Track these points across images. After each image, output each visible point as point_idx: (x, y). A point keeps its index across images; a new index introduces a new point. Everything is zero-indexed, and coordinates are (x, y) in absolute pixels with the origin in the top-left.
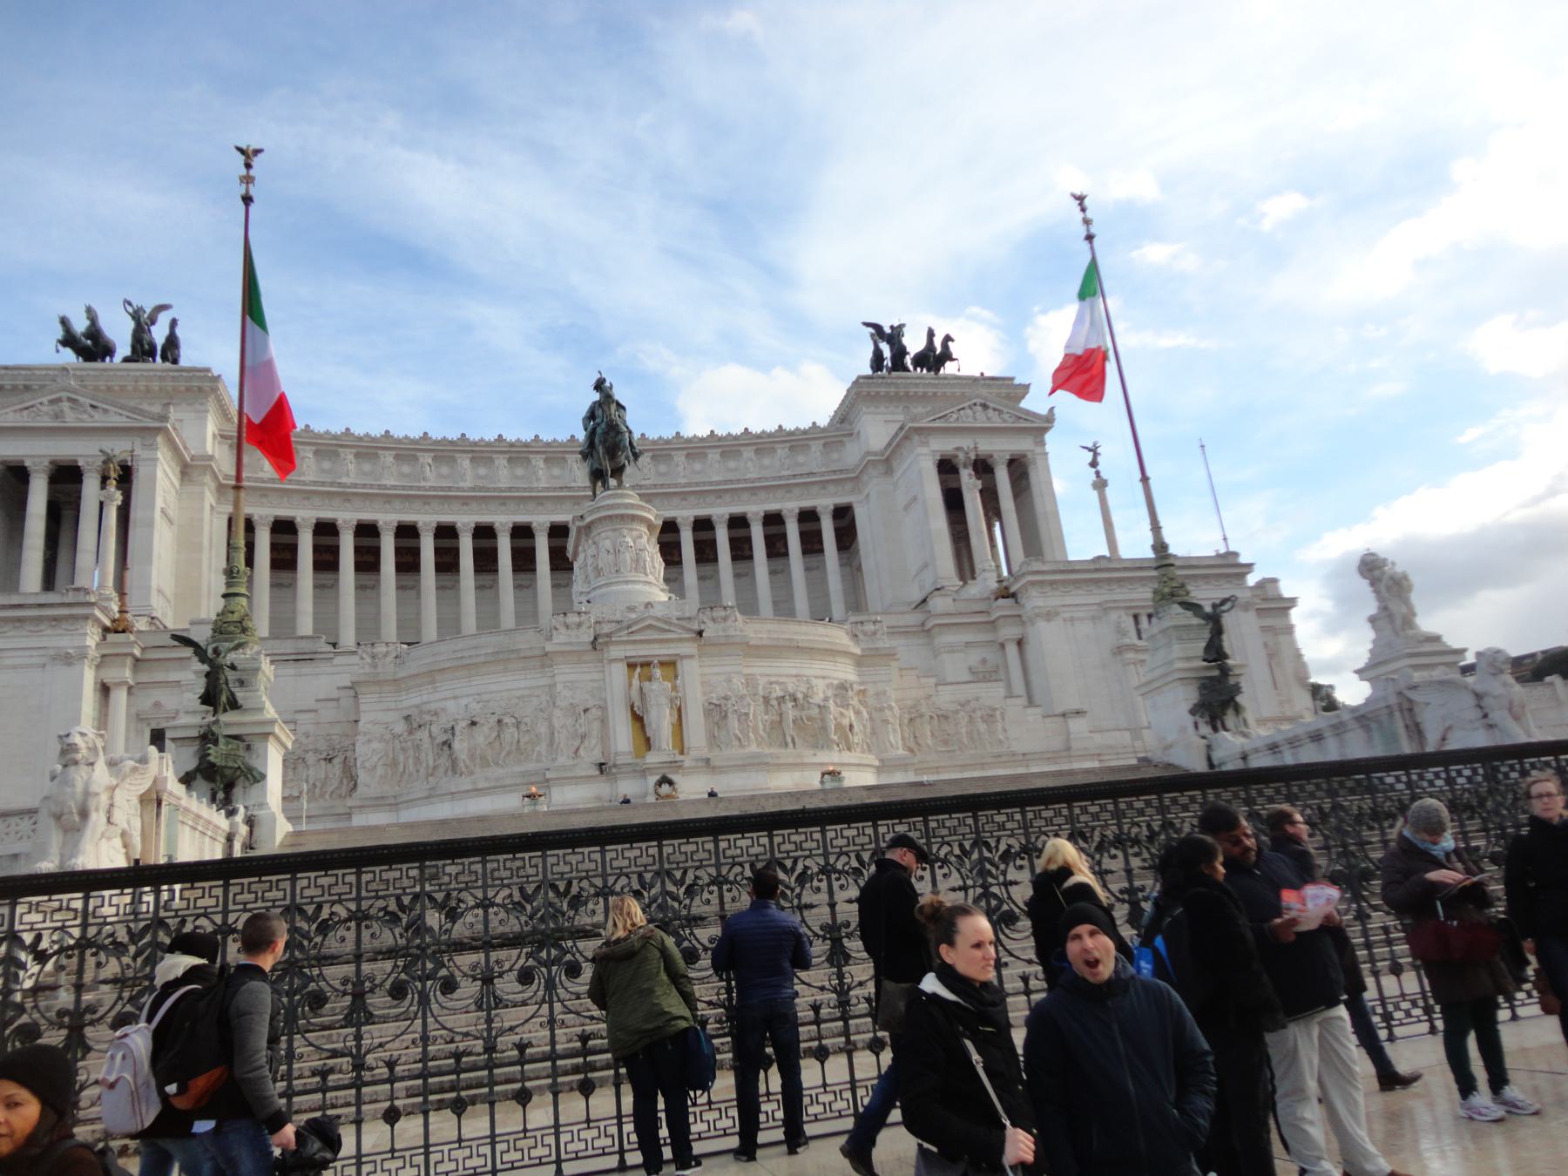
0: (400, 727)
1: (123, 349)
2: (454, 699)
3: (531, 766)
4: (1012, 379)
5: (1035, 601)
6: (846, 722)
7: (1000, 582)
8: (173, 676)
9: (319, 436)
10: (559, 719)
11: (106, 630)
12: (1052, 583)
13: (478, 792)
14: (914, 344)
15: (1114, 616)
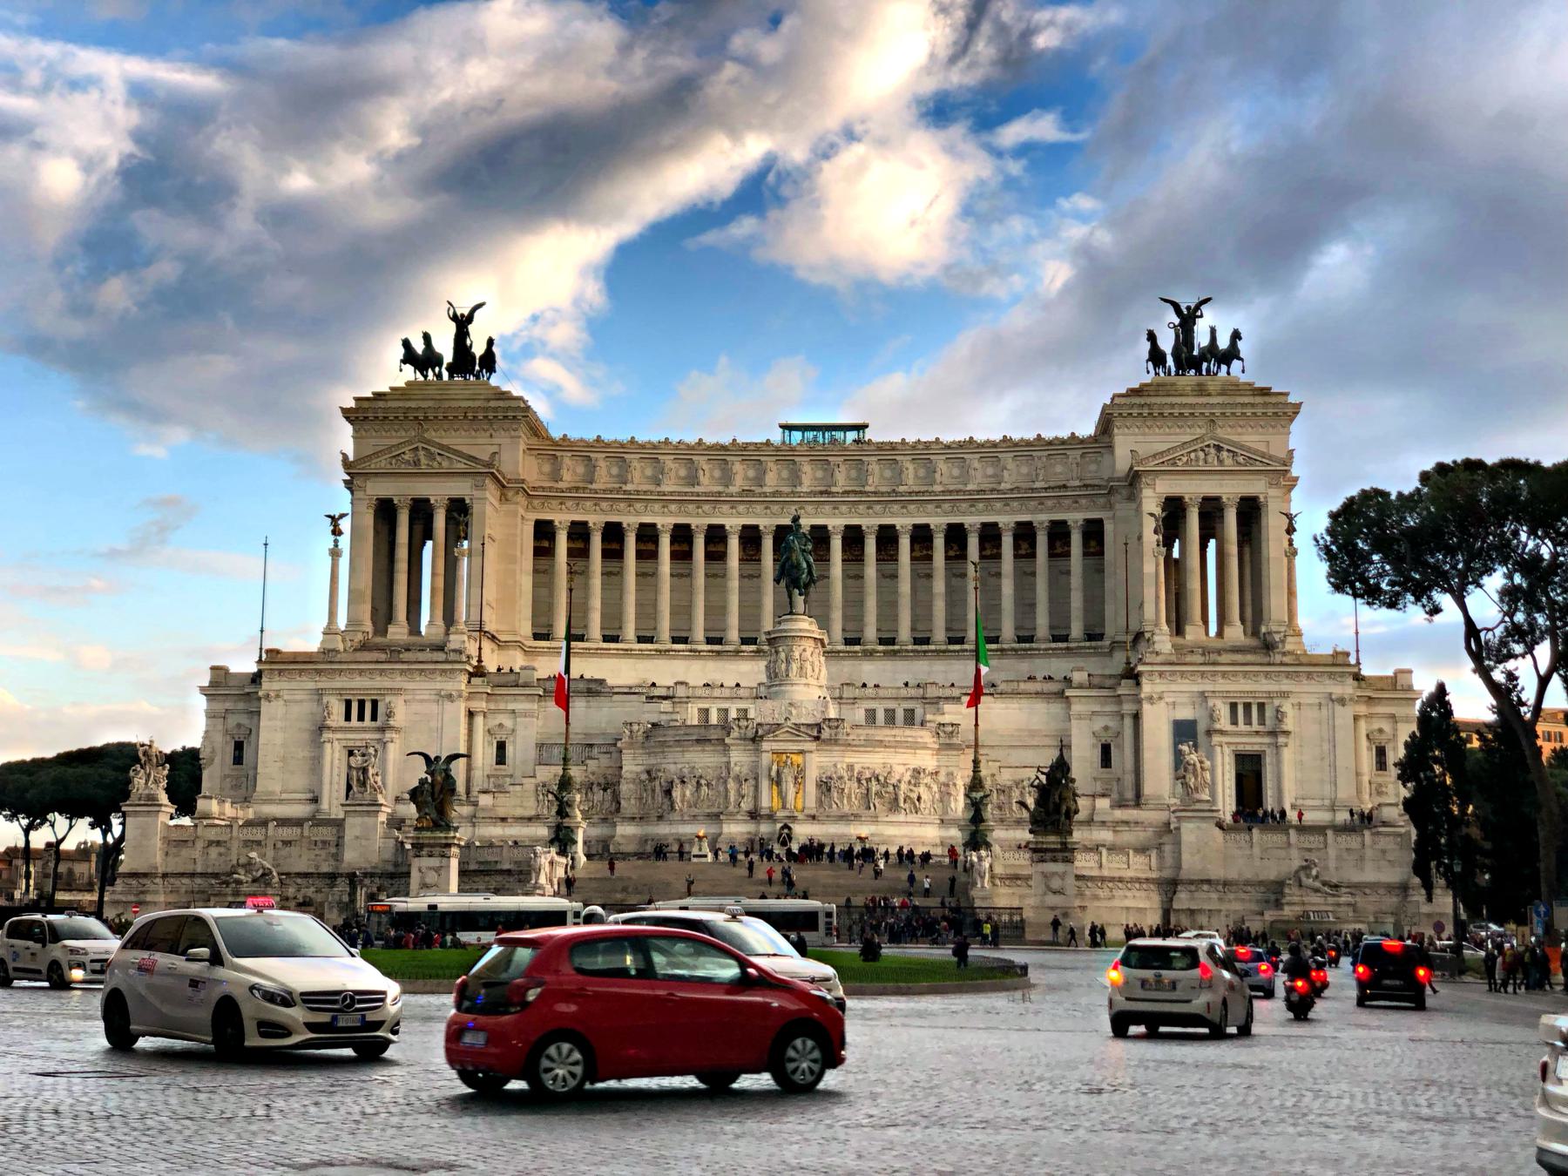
0: (644, 777)
1: (448, 357)
2: (675, 763)
3: (715, 810)
4: (1287, 394)
5: (1147, 688)
6: (915, 796)
7: (1128, 663)
8: (511, 706)
9: (608, 445)
10: (732, 785)
11: (471, 675)
12: (1161, 674)
13: (683, 822)
14: (1201, 339)
15: (1211, 703)
